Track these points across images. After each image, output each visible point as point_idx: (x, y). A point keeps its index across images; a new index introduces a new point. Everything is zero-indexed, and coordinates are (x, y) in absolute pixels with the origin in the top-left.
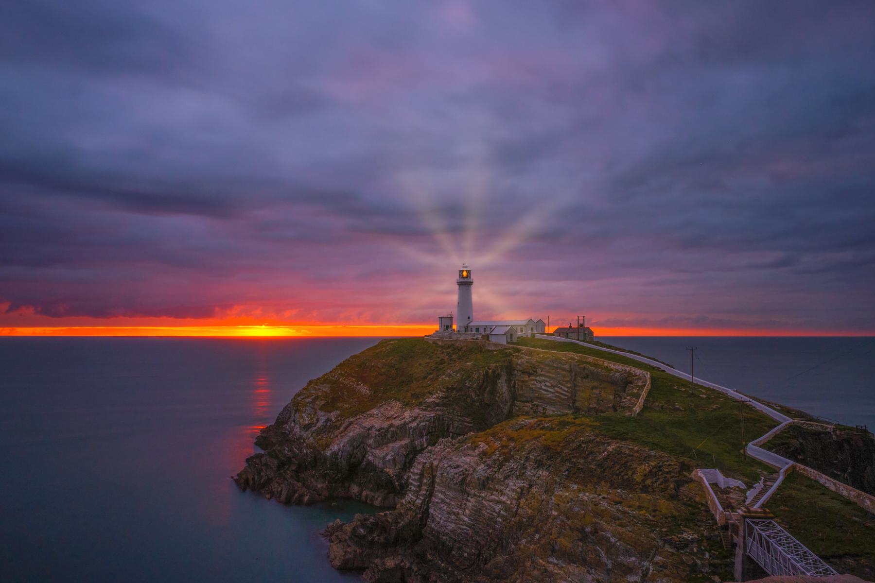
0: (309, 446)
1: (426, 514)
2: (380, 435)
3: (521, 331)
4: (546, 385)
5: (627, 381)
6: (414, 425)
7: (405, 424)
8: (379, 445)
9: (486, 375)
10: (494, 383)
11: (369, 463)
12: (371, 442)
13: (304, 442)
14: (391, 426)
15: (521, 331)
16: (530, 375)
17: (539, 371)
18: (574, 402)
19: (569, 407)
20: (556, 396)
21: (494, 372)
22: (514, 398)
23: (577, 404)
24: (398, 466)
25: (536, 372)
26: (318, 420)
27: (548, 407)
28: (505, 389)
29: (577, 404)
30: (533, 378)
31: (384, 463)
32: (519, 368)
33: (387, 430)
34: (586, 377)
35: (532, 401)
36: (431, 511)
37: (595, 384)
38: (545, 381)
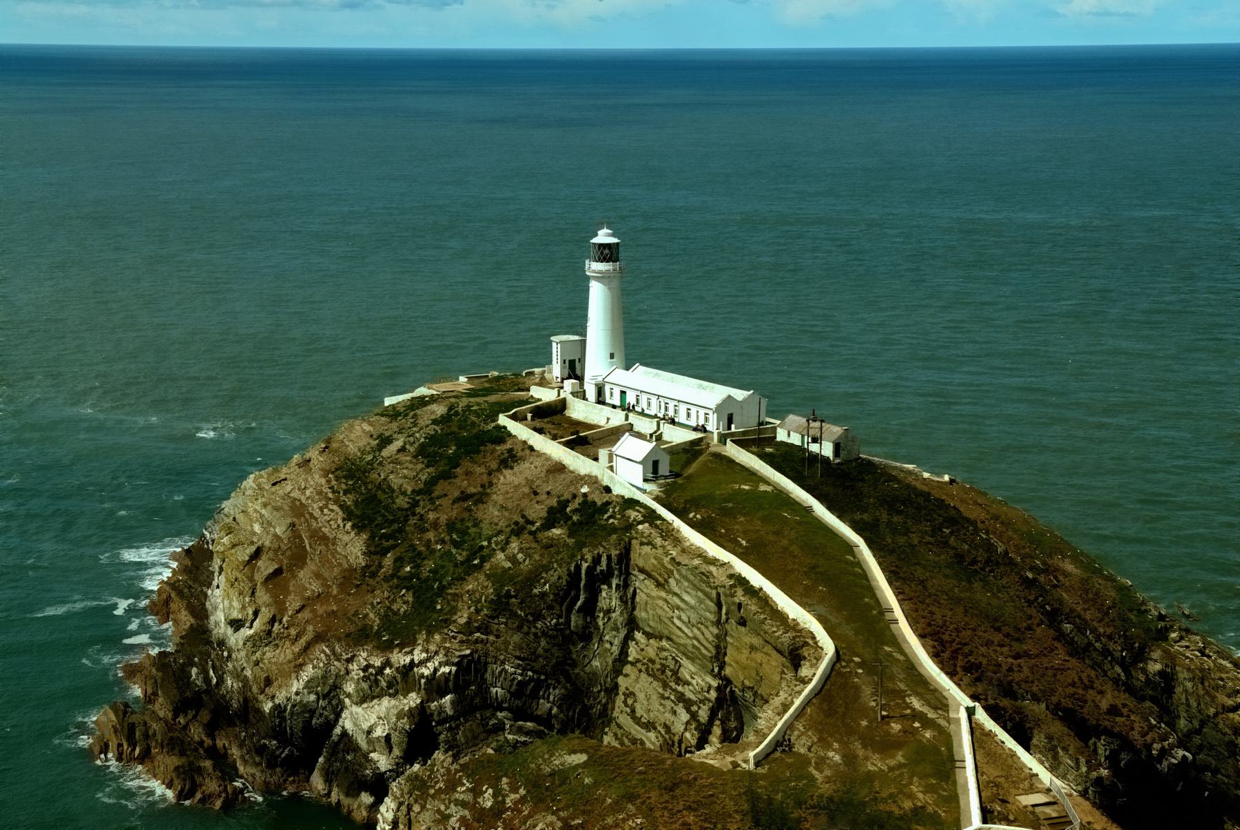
2: (365, 679)
3: (706, 420)
4: (679, 618)
5: (797, 652)
8: (364, 699)
9: (575, 576)
11: (344, 733)
13: (230, 656)
14: (387, 663)
15: (706, 420)
16: (659, 585)
17: (671, 580)
18: (722, 666)
20: (694, 646)
21: (590, 570)
23: (728, 671)
24: (396, 752)
25: (666, 581)
26: (256, 614)
27: (685, 662)
29: (728, 671)
30: (663, 594)
32: (641, 563)
33: (380, 671)
34: (742, 622)
35: (661, 639)
37: (756, 641)
38: (678, 608)
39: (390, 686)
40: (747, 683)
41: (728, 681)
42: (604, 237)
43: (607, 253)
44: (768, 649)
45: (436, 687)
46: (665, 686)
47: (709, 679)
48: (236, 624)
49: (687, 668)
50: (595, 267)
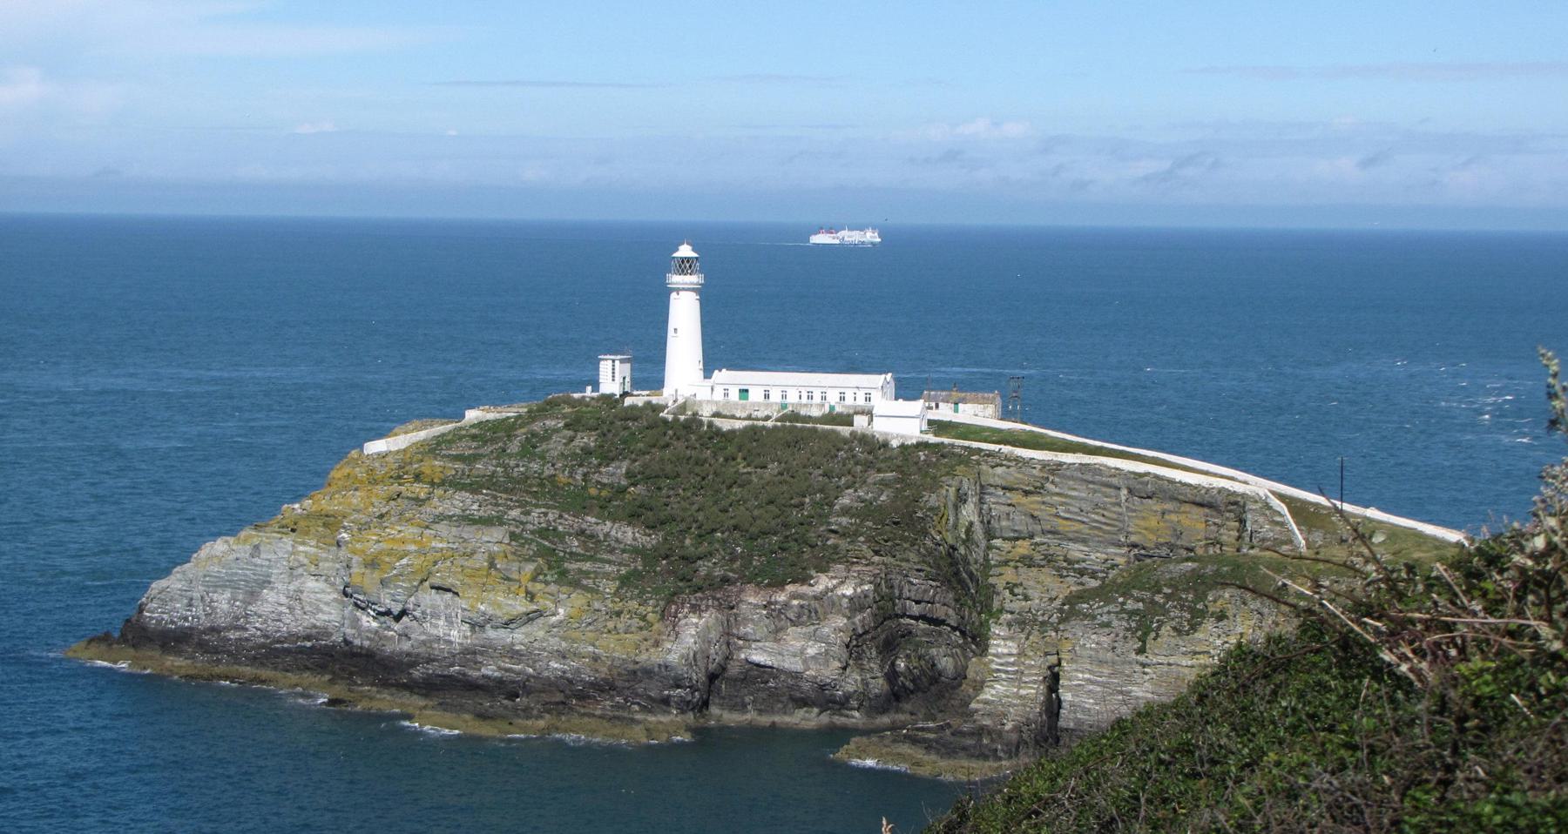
0: (563, 656)
1: (1053, 706)
6: (848, 591)
7: (827, 590)
10: (956, 508)
12: (749, 629)
16: (1027, 493)
19: (1120, 545)
22: (990, 534)
23: (1133, 538)
27: (1071, 545)
28: (975, 519)
31: (805, 662)
33: (786, 605)
35: (1032, 537)
36: (1066, 696)
37: (1169, 506)
39: (799, 617)
40: (1161, 540)
41: (1135, 546)
42: (685, 251)
43: (685, 266)
44: (1187, 507)
45: (856, 604)
46: (1058, 569)
47: (1112, 550)
48: (529, 618)
49: (1076, 551)
50: (676, 279)
